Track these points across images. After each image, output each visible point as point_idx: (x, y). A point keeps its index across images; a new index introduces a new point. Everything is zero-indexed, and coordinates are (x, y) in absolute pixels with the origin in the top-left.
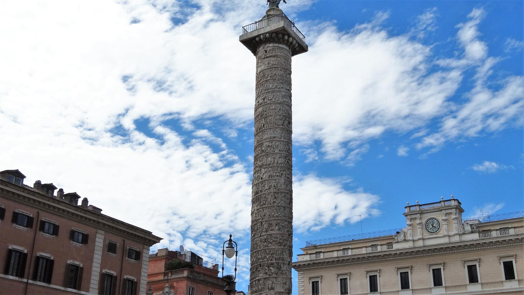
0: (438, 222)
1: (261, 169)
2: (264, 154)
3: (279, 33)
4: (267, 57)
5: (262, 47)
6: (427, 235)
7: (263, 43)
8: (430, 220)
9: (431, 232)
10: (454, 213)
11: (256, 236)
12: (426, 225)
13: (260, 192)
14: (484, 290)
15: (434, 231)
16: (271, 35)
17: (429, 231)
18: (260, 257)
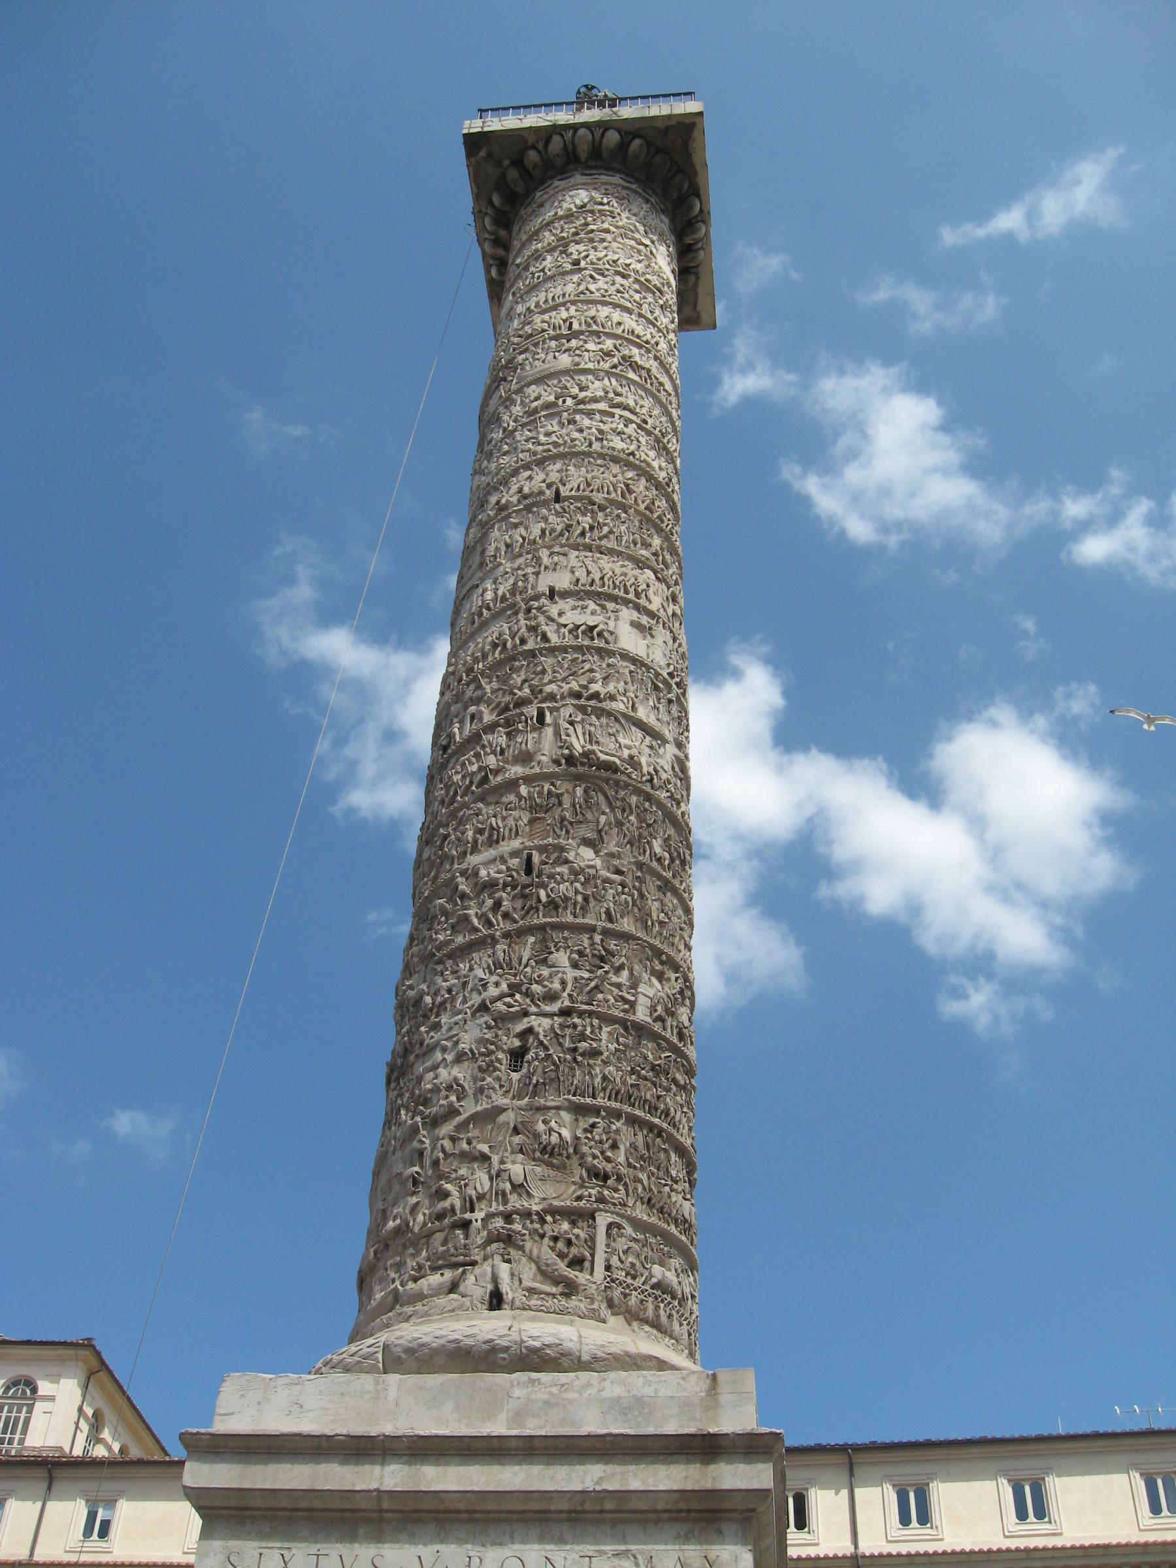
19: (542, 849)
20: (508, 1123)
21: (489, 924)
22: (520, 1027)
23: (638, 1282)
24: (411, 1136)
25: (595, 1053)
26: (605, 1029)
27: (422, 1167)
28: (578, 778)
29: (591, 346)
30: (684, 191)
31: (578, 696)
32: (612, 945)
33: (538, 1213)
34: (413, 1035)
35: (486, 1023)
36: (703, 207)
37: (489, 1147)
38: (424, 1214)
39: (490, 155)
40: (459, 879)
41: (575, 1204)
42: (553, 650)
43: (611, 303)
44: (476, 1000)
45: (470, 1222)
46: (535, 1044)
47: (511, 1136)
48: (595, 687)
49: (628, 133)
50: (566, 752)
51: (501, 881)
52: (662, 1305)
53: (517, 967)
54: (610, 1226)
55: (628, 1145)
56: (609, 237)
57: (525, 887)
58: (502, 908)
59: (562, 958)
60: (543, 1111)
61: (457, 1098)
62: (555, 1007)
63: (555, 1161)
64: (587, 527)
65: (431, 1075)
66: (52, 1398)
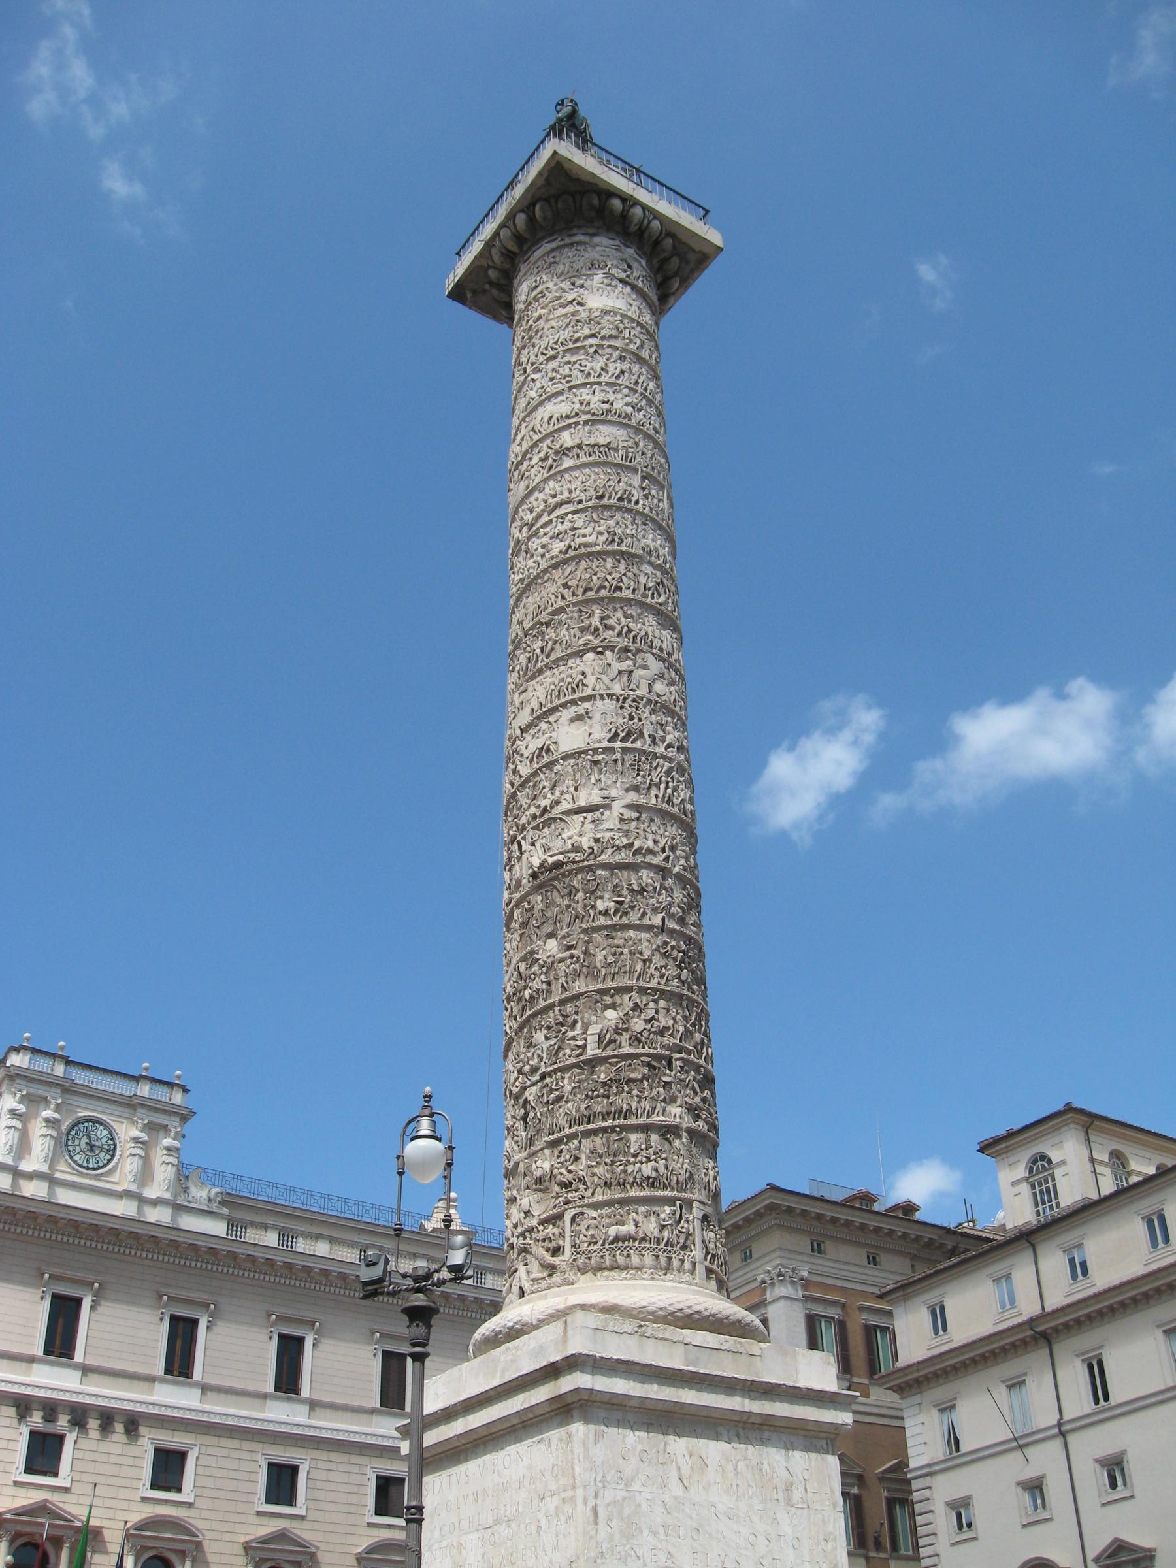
0: (112, 1139)
1: (639, 651)
2: (649, 600)
3: (678, 255)
4: (634, 287)
5: (611, 242)
6: (63, 1171)
7: (617, 233)
8: (86, 1124)
9: (81, 1166)
10: (173, 1130)
11: (634, 918)
12: (68, 1133)
13: (649, 741)
14: (208, 1407)
15: (91, 1166)
16: (664, 231)
17: (75, 1158)
18: (665, 1021)
19: (524, 959)
22: (521, 1101)
23: (599, 1246)
25: (559, 1099)
26: (567, 1076)
28: (540, 887)
29: (535, 459)
30: (598, 206)
31: (534, 817)
32: (569, 1008)
36: (624, 196)
39: (474, 292)
41: (555, 1211)
42: (523, 785)
43: (545, 399)
48: (545, 803)
49: (528, 207)
50: (530, 871)
52: (618, 1252)
54: (573, 1219)
55: (588, 1151)
56: (541, 323)
59: (539, 1037)
62: (537, 1077)
63: (542, 1187)
64: (538, 651)
66: (1063, 1162)
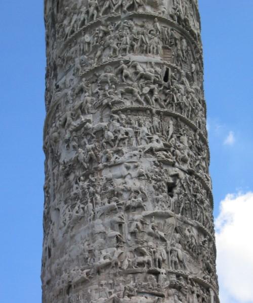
19: (173, 69)
20: (173, 225)
21: (147, 101)
24: (109, 212)
27: (122, 232)
33: (190, 279)
34: (99, 152)
35: (154, 162)
37: (165, 234)
38: (129, 261)
40: (123, 65)
44: (148, 147)
45: (159, 273)
46: (180, 185)
47: (174, 232)
51: (153, 78)
53: (167, 136)
57: (165, 88)
58: (155, 96)
60: (186, 225)
61: (142, 199)
65: (120, 181)
